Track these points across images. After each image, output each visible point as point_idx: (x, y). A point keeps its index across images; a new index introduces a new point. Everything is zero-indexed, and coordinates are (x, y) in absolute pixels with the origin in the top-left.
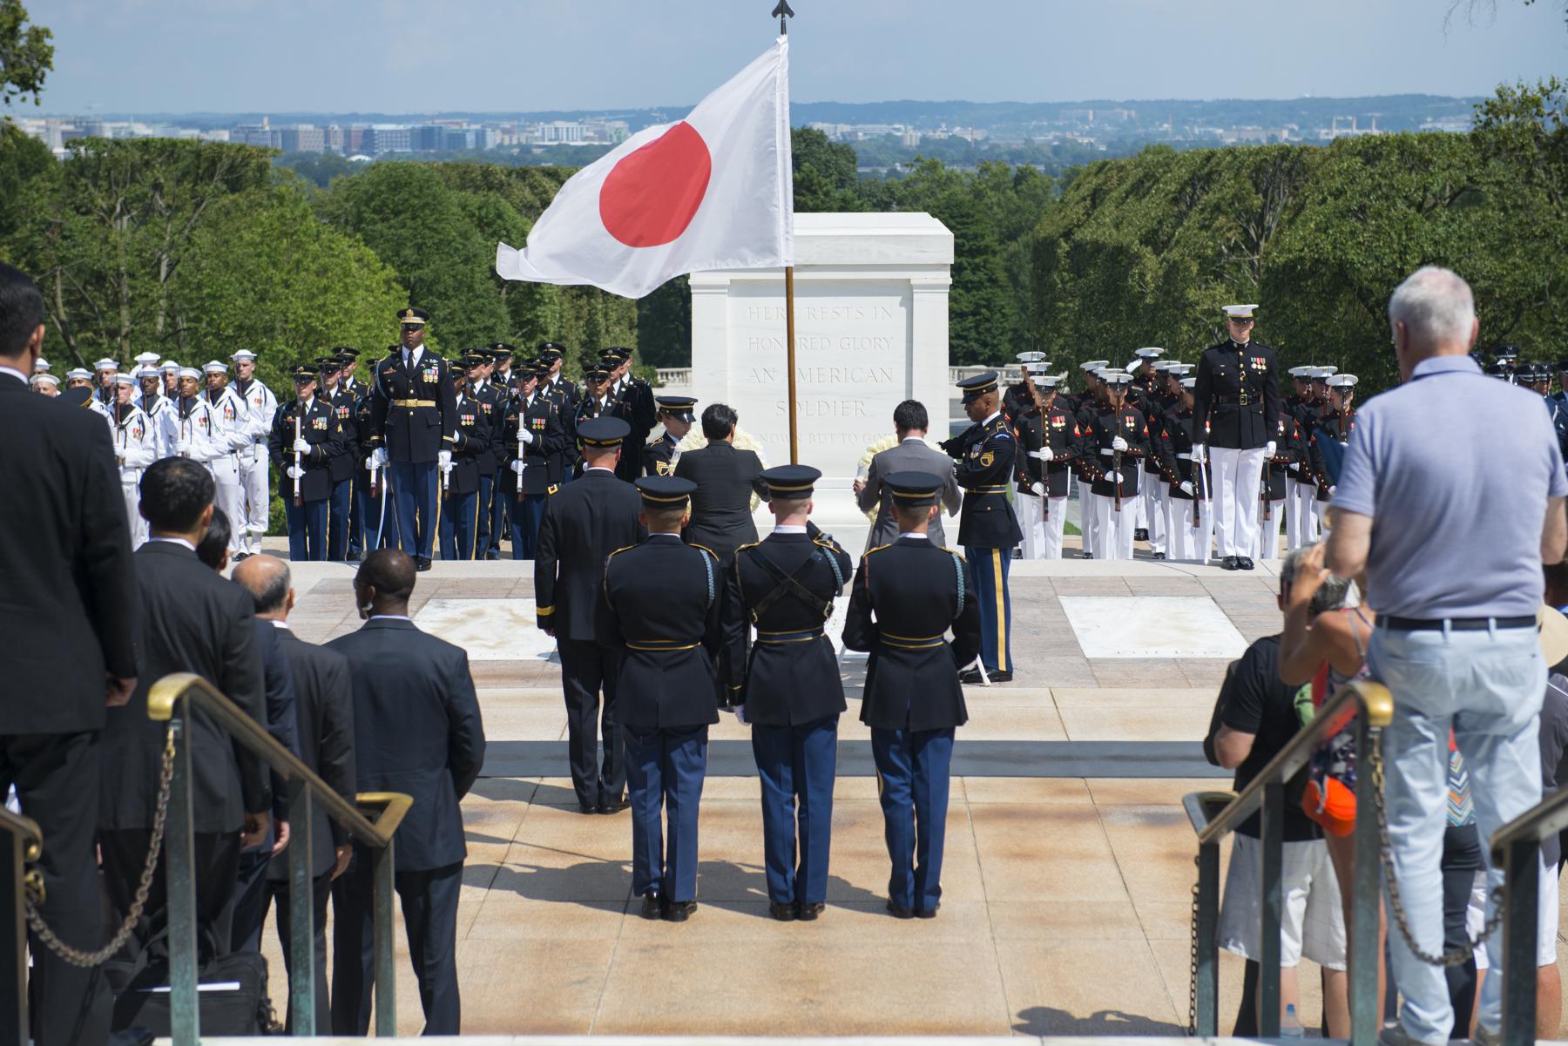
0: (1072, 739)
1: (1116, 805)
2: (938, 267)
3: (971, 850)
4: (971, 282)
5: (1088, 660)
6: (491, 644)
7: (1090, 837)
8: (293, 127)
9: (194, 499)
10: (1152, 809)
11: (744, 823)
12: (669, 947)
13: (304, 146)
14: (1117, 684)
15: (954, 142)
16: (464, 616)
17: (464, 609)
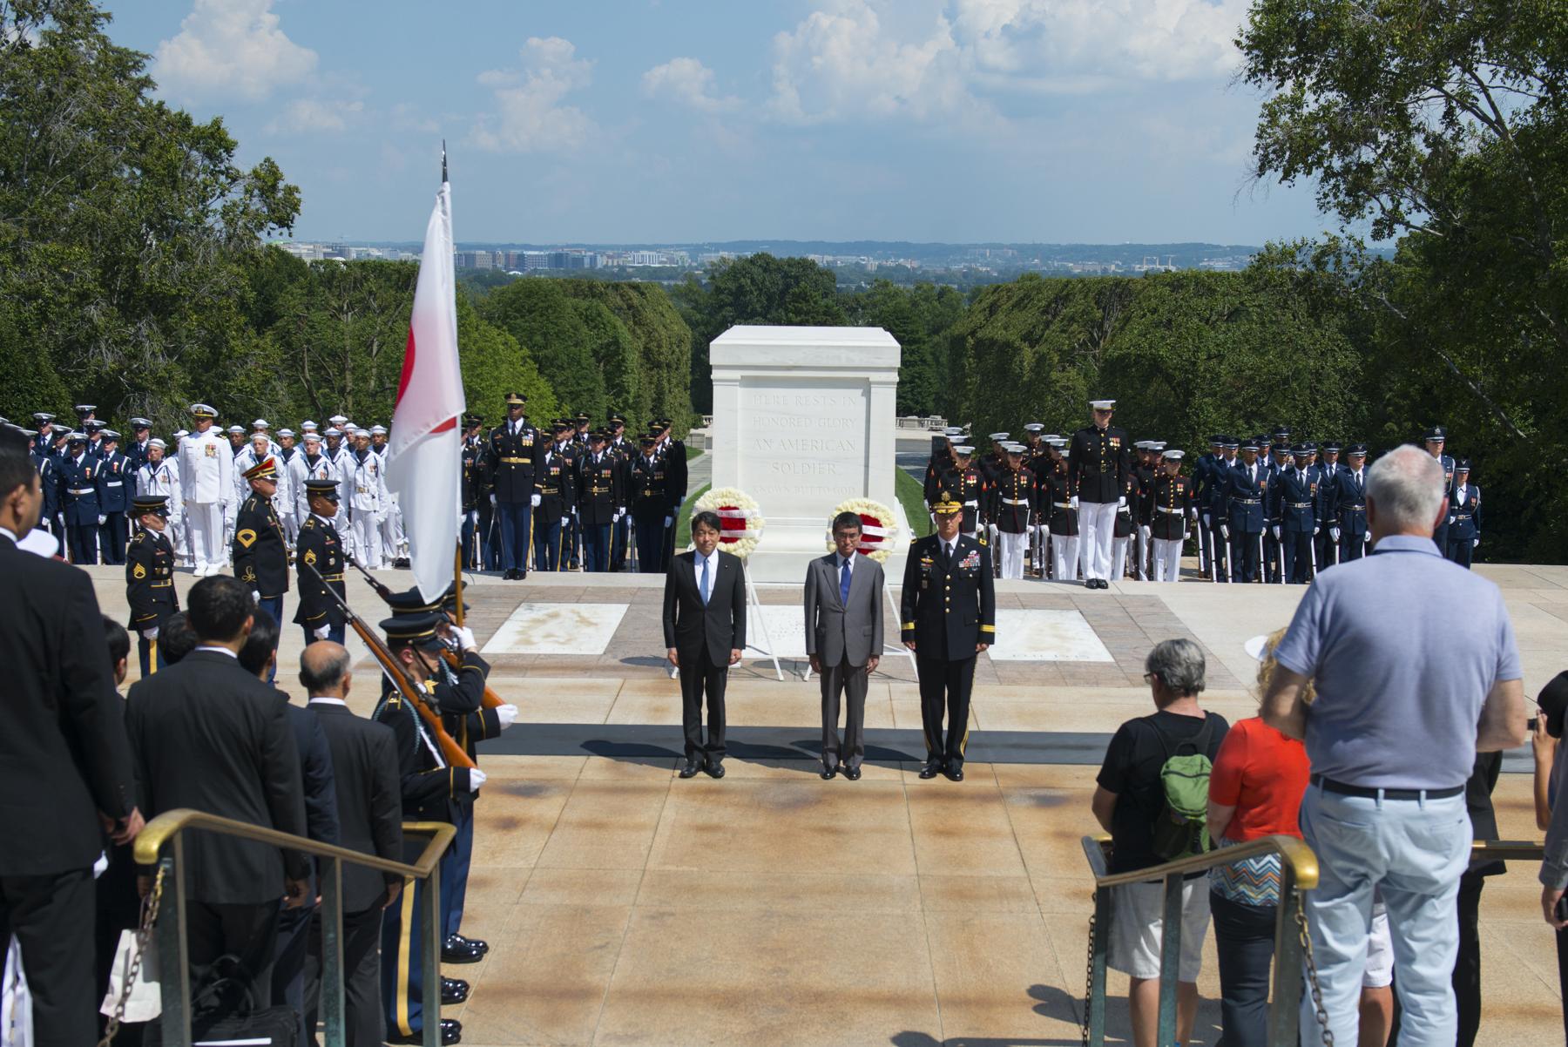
0: (982, 729)
1: (1015, 788)
2: (890, 369)
3: (906, 827)
4: (910, 362)
5: (992, 661)
6: (562, 640)
7: (996, 818)
8: (473, 252)
9: (238, 612)
10: (1042, 792)
11: (737, 800)
12: (672, 914)
13: (478, 265)
14: (1014, 682)
15: (900, 268)
16: (545, 617)
17: (546, 612)
